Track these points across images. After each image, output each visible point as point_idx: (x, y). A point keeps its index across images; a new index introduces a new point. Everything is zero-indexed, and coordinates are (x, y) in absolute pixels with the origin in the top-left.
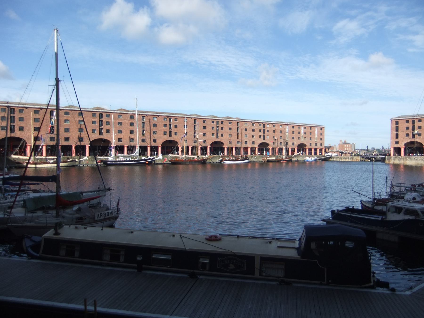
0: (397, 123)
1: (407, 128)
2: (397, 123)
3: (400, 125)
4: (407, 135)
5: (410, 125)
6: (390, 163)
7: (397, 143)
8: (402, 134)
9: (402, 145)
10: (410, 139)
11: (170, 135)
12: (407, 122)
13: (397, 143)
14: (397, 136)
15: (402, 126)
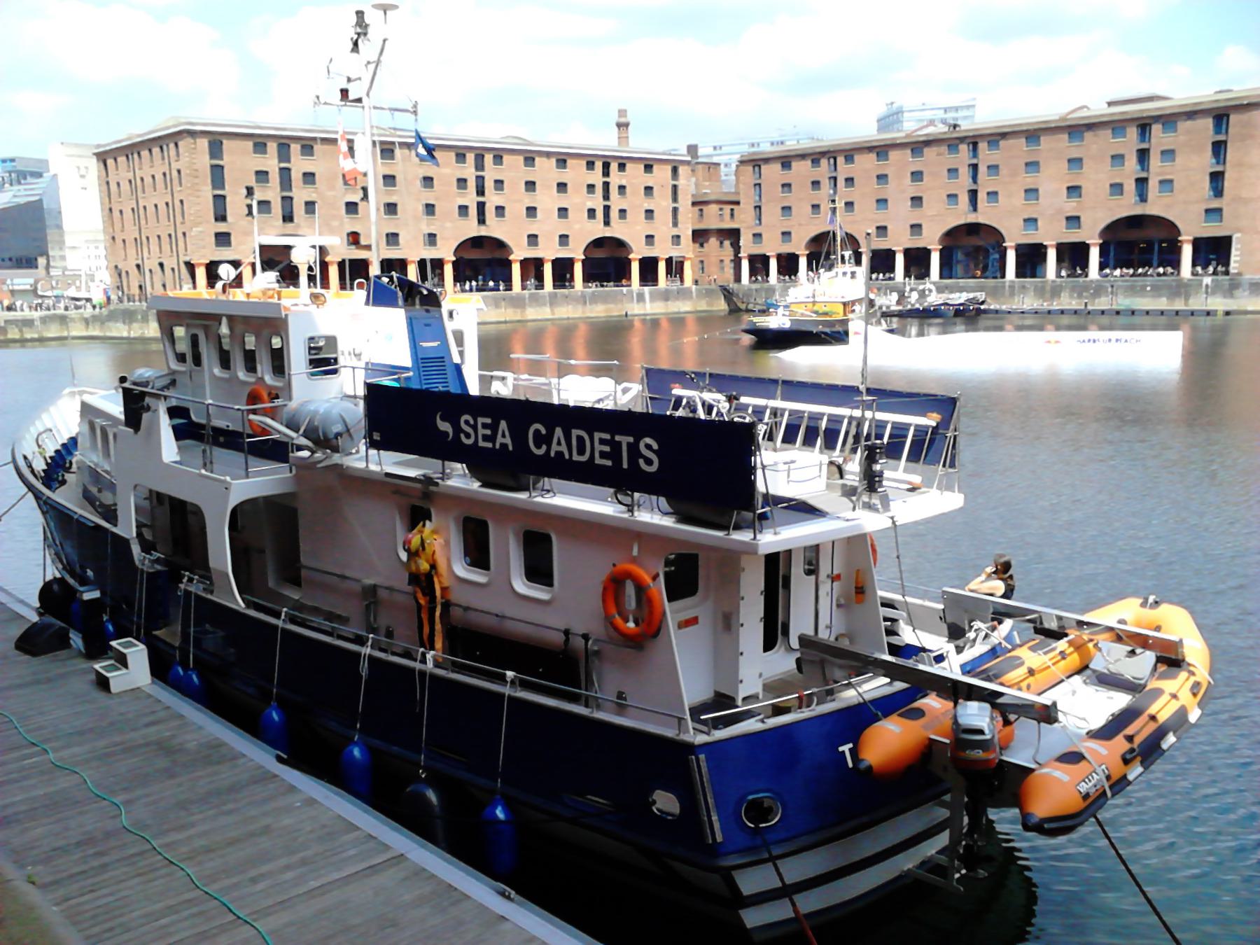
11: (482, 220)
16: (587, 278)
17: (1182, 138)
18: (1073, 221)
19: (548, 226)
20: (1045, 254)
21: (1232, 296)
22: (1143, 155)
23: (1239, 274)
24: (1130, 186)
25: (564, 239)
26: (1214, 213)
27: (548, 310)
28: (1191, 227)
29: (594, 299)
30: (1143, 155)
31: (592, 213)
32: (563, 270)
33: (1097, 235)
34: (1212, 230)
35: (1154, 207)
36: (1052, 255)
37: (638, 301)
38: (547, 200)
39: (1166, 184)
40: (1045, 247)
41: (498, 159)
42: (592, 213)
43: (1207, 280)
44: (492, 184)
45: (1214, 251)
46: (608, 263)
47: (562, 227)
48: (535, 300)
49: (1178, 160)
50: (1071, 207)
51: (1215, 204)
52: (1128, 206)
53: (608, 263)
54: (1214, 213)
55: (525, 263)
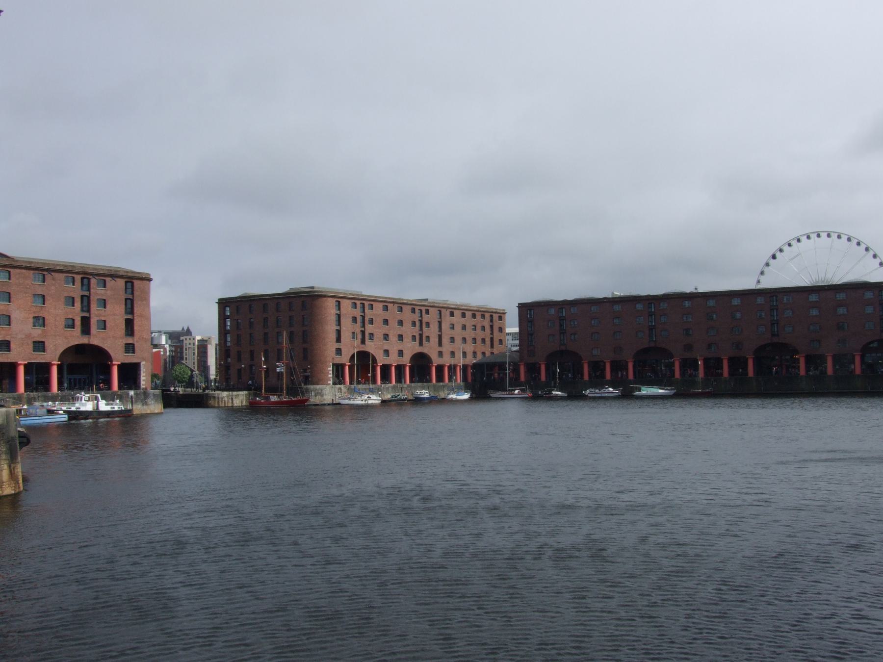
17: (109, 292)
18: (39, 346)
20: (540, 368)
21: (146, 404)
22: (86, 301)
23: (146, 389)
24: (78, 323)
26: (130, 348)
28: (119, 357)
30: (86, 301)
33: (57, 357)
34: (130, 359)
35: (96, 339)
36: (21, 371)
39: (103, 325)
40: (13, 366)
43: (132, 393)
45: (130, 375)
49: (108, 306)
50: (37, 333)
51: (130, 340)
52: (76, 338)
54: (130, 348)
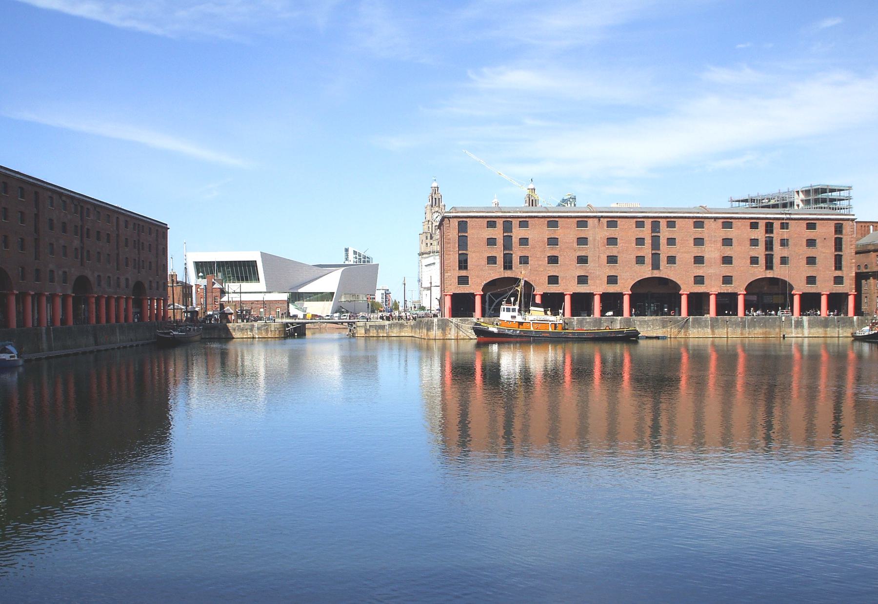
0: (463, 226)
1: (491, 242)
2: (463, 226)
3: (471, 233)
4: (492, 260)
5: (498, 233)
6: (449, 336)
7: (463, 280)
8: (477, 256)
9: (475, 287)
10: (498, 272)
12: (491, 224)
13: (463, 280)
14: (463, 264)
15: (478, 234)
16: (747, 307)
19: (713, 272)
25: (727, 280)
27: (709, 330)
29: (753, 324)
31: (754, 261)
32: (727, 304)
37: (796, 327)
38: (712, 252)
41: (671, 224)
42: (754, 261)
44: (665, 241)
46: (768, 296)
47: (726, 270)
48: (698, 324)
53: (768, 296)
55: (691, 297)
